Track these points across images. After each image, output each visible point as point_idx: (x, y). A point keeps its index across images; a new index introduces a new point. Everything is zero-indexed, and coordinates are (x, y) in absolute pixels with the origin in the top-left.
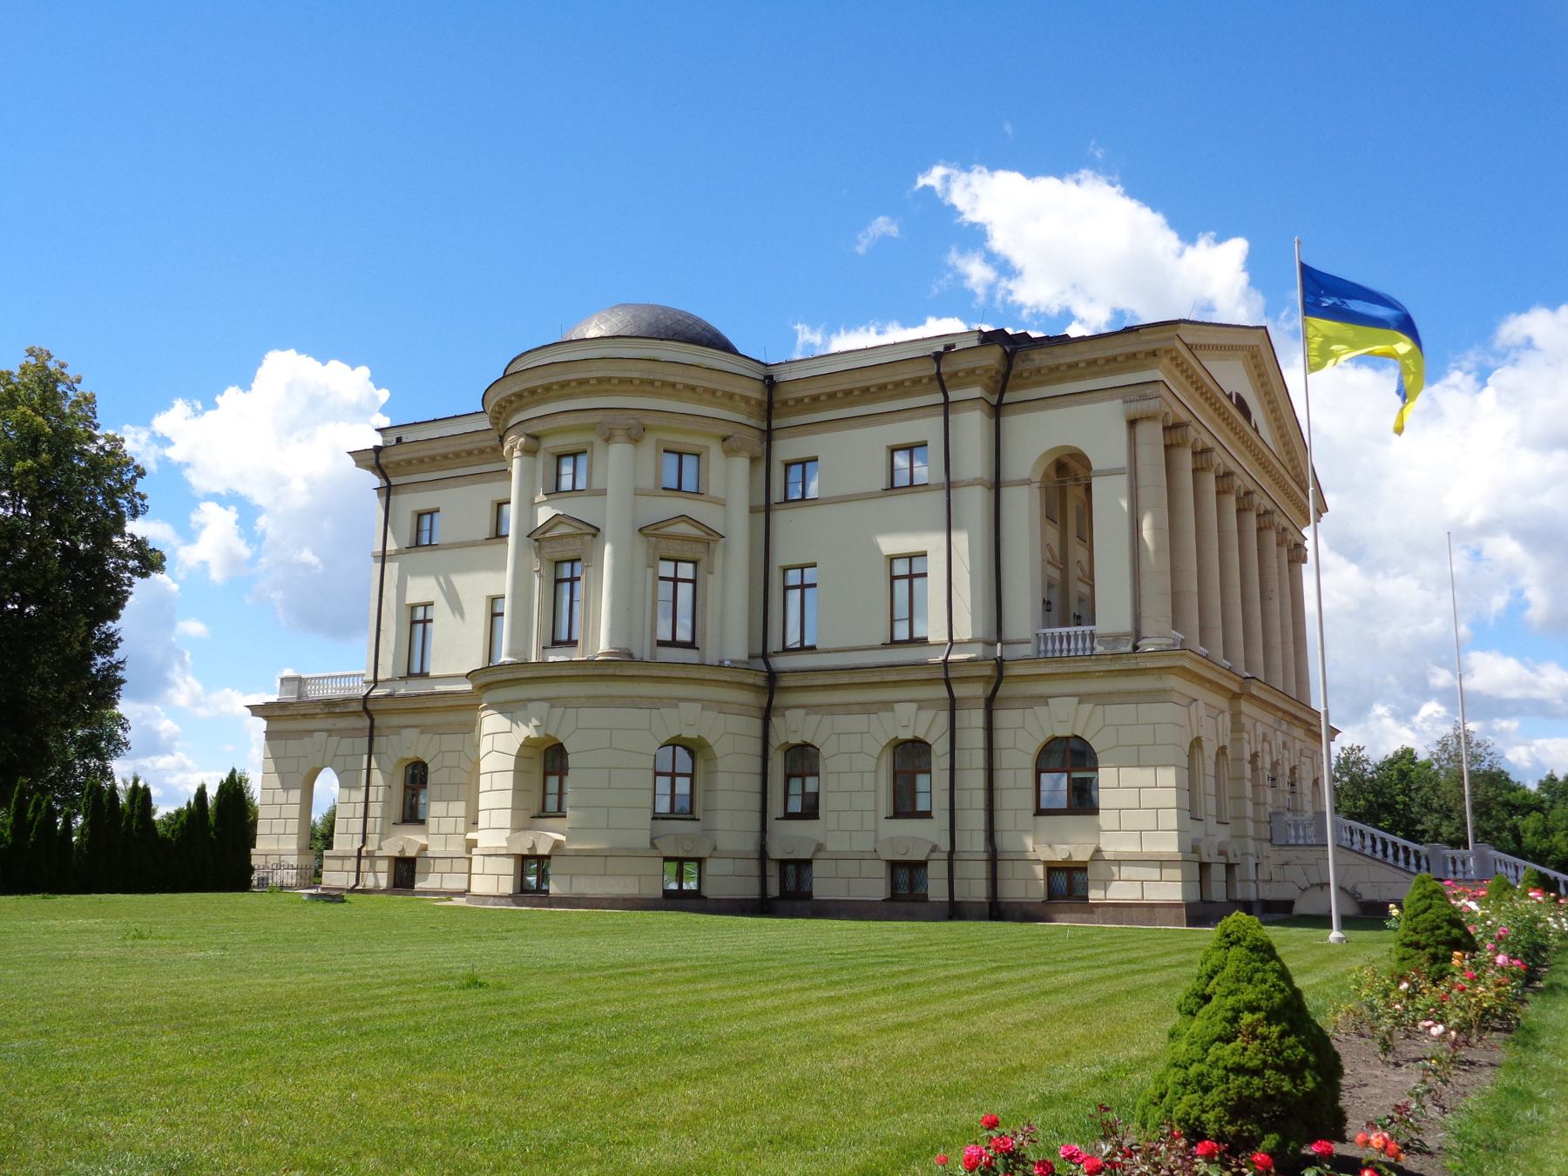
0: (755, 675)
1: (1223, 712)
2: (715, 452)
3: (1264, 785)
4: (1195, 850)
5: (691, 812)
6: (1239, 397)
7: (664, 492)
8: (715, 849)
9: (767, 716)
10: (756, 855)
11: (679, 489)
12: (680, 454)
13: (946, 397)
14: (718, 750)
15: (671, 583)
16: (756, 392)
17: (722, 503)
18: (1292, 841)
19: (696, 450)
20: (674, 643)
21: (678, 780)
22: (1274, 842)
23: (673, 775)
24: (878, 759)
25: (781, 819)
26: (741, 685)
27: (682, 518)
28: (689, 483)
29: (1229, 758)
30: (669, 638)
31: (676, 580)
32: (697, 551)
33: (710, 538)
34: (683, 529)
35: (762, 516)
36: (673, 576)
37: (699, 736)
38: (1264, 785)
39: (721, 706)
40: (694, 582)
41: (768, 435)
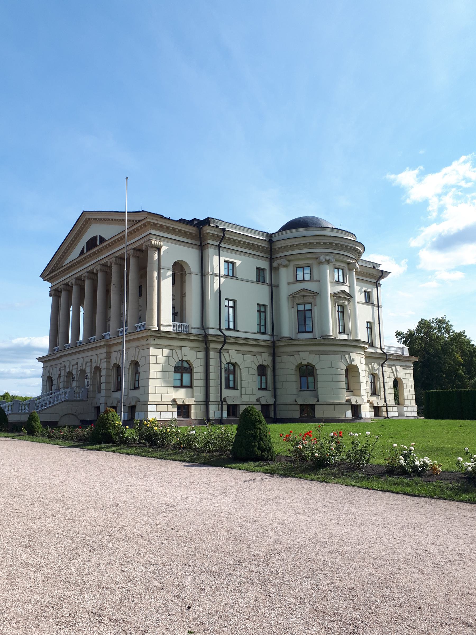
5: (315, 389)
7: (296, 282)
8: (318, 401)
11: (304, 280)
12: (303, 268)
14: (317, 367)
17: (319, 281)
19: (310, 265)
20: (306, 332)
27: (302, 290)
28: (307, 277)
30: (304, 330)
32: (310, 300)
34: (303, 293)
37: (308, 363)
40: (311, 310)
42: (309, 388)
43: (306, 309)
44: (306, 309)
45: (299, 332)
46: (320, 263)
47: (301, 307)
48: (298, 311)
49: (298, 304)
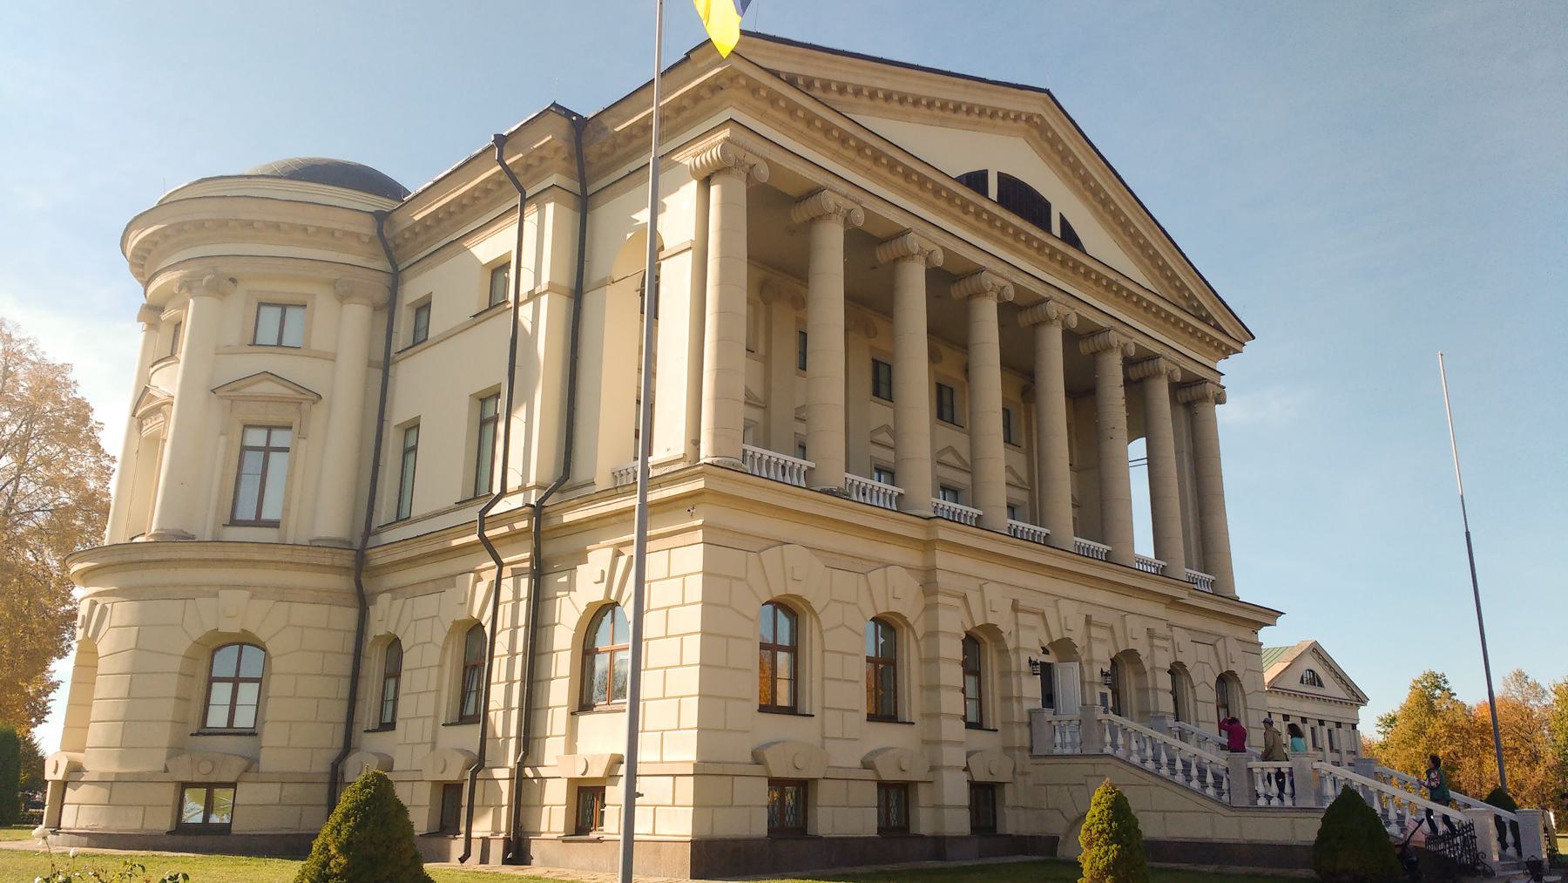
0: (293, 550)
1: (886, 565)
2: (324, 304)
3: (1019, 673)
4: (757, 758)
6: (1004, 179)
9: (363, 602)
10: (327, 779)
11: (279, 344)
12: (284, 307)
13: (523, 192)
15: (262, 454)
16: (366, 228)
18: (1058, 751)
20: (258, 522)
21: (242, 686)
22: (1035, 753)
23: (236, 681)
24: (444, 649)
25: (374, 731)
26: (319, 568)
27: (262, 376)
29: (920, 634)
31: (267, 450)
33: (302, 397)
35: (380, 373)
36: (263, 444)
38: (1019, 673)
39: (283, 594)
41: (395, 281)
42: (236, 725)
43: (272, 445)
44: (272, 445)
45: (234, 522)
46: (343, 298)
47: (257, 438)
48: (244, 449)
49: (246, 426)
